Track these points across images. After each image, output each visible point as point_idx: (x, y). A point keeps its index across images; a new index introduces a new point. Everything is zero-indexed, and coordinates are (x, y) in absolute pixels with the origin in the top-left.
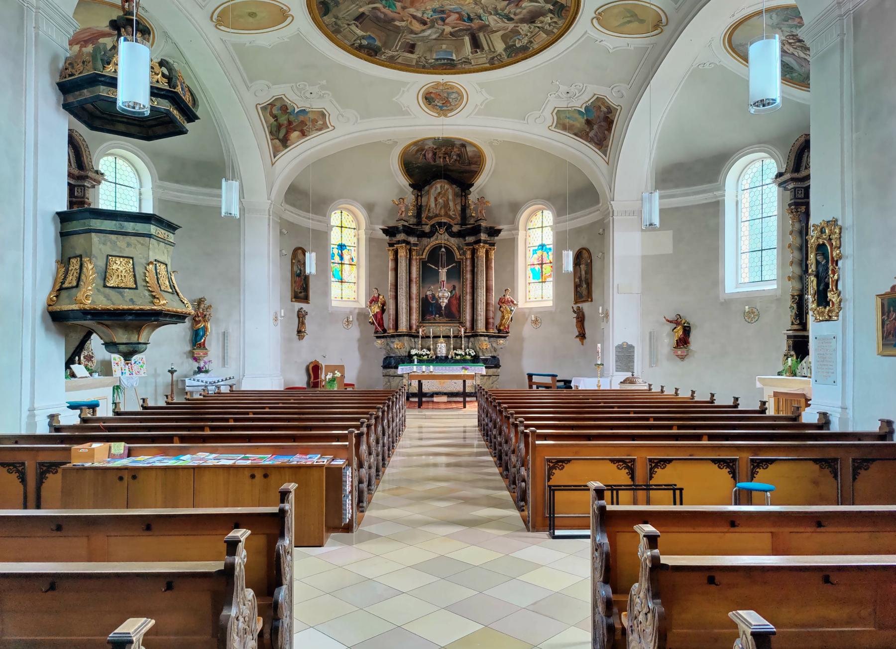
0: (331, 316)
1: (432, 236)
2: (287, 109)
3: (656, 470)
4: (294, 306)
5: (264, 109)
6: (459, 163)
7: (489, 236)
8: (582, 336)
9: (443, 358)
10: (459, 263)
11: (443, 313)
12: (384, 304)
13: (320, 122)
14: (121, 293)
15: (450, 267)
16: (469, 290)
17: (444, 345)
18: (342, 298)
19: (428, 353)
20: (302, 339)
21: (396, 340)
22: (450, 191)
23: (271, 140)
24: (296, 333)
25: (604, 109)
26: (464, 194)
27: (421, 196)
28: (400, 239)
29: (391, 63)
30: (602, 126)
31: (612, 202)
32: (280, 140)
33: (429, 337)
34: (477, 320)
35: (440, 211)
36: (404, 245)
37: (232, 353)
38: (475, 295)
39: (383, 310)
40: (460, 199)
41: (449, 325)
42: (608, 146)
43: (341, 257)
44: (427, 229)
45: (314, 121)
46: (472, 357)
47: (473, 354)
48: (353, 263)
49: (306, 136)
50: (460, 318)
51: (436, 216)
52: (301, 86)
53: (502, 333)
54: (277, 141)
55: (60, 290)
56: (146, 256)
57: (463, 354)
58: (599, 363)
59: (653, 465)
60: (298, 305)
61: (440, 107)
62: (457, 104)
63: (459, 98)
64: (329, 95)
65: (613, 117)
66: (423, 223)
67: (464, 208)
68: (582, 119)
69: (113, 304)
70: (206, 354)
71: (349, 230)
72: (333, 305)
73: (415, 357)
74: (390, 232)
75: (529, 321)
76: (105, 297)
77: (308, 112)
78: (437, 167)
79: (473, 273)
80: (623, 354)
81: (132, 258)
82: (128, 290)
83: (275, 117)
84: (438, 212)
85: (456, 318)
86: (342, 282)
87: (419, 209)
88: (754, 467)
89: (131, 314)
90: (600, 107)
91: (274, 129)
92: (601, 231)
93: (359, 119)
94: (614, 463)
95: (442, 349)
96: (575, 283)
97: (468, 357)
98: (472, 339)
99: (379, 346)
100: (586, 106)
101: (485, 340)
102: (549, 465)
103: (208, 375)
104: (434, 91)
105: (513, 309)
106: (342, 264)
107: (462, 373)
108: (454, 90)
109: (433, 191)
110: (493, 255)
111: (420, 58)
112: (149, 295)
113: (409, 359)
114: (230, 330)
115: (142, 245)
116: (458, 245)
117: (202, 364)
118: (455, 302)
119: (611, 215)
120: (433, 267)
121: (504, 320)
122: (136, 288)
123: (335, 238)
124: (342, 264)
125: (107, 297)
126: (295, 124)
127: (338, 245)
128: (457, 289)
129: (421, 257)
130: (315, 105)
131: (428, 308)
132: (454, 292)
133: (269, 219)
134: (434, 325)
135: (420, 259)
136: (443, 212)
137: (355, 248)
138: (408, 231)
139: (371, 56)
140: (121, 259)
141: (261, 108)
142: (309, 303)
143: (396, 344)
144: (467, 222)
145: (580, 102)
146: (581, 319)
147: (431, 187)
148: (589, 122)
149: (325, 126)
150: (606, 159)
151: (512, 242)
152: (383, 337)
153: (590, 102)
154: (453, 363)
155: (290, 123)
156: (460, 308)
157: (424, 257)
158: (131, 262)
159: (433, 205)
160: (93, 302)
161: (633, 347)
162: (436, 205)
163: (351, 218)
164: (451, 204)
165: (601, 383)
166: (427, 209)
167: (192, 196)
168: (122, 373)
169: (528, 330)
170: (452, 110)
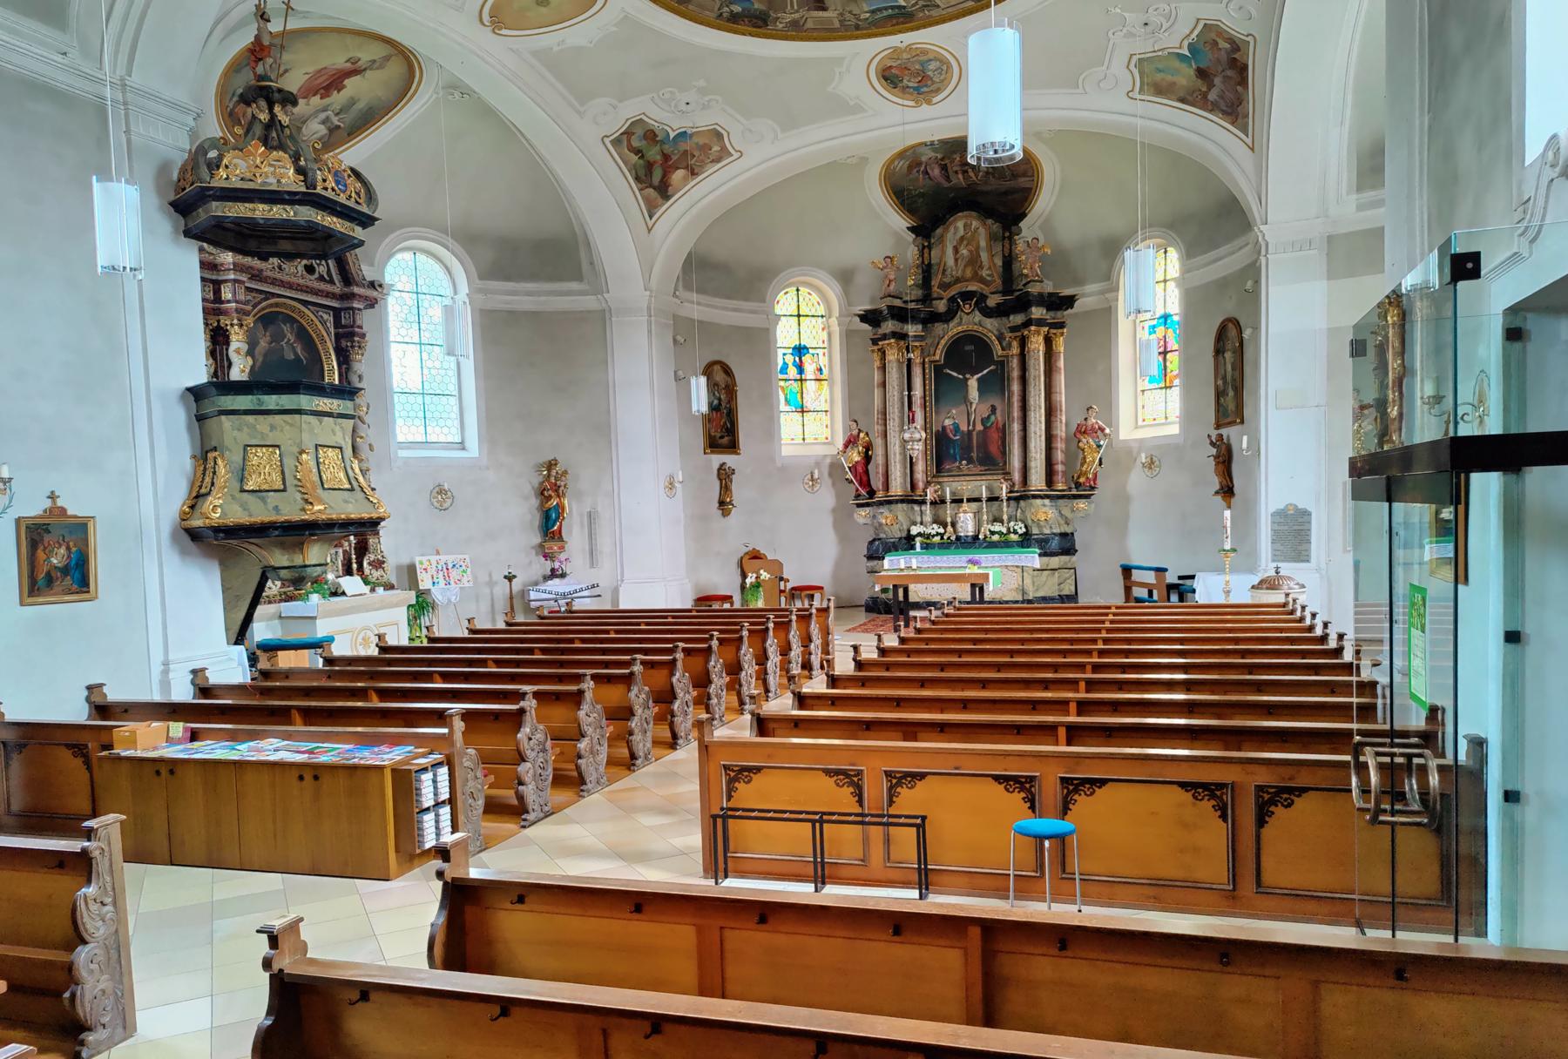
0: (784, 473)
1: (952, 318)
2: (655, 135)
3: (899, 790)
4: (710, 461)
5: (616, 142)
6: (994, 177)
7: (1047, 310)
8: (1227, 491)
10: (1002, 364)
12: (868, 447)
13: (716, 148)
14: (263, 500)
15: (985, 372)
16: (1016, 413)
17: (970, 516)
18: (804, 439)
19: (942, 531)
20: (729, 514)
21: (884, 510)
22: (982, 231)
23: (641, 190)
24: (717, 505)
25: (1224, 45)
26: (1007, 234)
27: (930, 247)
28: (887, 331)
29: (797, 31)
30: (1227, 77)
31: (1262, 227)
32: (655, 188)
35: (964, 271)
36: (893, 341)
37: (604, 543)
39: (867, 459)
40: (1001, 244)
41: (984, 478)
42: (1247, 116)
43: (800, 368)
44: (941, 306)
45: (705, 148)
48: (823, 377)
49: (697, 174)
51: (958, 280)
52: (667, 96)
53: (1082, 489)
54: (651, 190)
55: (197, 498)
56: (297, 441)
58: (1228, 546)
59: (894, 781)
60: (717, 459)
61: (914, 88)
62: (945, 79)
63: (945, 67)
64: (717, 102)
65: (1245, 57)
66: (935, 295)
67: (1009, 261)
68: (1187, 69)
69: (250, 516)
70: (562, 548)
71: (814, 319)
72: (783, 454)
73: (918, 540)
74: (871, 318)
76: (241, 506)
77: (691, 136)
78: (955, 189)
79: (1024, 380)
80: (1286, 528)
81: (278, 446)
82: (272, 493)
83: (638, 152)
84: (959, 274)
86: (803, 412)
87: (927, 271)
88: (1069, 792)
89: (276, 528)
90: (1215, 43)
91: (642, 173)
92: (1249, 284)
93: (779, 130)
94: (830, 777)
95: (967, 523)
96: (1217, 387)
97: (1013, 537)
98: (1022, 503)
99: (861, 521)
100: (1190, 44)
101: (1044, 505)
102: (729, 775)
103: (565, 580)
104: (894, 64)
105: (1102, 443)
106: (801, 380)
107: (967, 571)
108: (931, 56)
109: (950, 235)
110: (1060, 345)
111: (842, 14)
112: (303, 499)
113: (907, 543)
114: (599, 509)
115: (291, 425)
116: (998, 330)
117: (557, 565)
119: (1263, 252)
120: (955, 374)
122: (284, 490)
123: (786, 336)
124: (801, 380)
125: (244, 507)
126: (675, 158)
127: (794, 348)
129: (933, 358)
130: (701, 121)
131: (944, 451)
132: (993, 418)
133: (650, 323)
134: (957, 479)
135: (931, 362)
136: (969, 273)
137: (826, 350)
138: (900, 315)
139: (760, 27)
140: (264, 449)
141: (610, 142)
142: (739, 454)
143: (885, 516)
144: (1014, 287)
145: (1176, 37)
146: (1225, 459)
147: (947, 230)
148: (1202, 73)
149: (724, 153)
150: (1249, 141)
151: (1105, 317)
152: (867, 505)
153: (1194, 35)
154: (985, 547)
155: (666, 157)
156: (1004, 447)
157: (937, 358)
158: (278, 452)
159: (950, 261)
160: (224, 514)
161: (1309, 514)
162: (956, 260)
163: (815, 297)
164: (984, 256)
165: (1231, 586)
166: (941, 269)
167: (531, 298)
168: (434, 583)
169: (1137, 480)
170: (938, 91)
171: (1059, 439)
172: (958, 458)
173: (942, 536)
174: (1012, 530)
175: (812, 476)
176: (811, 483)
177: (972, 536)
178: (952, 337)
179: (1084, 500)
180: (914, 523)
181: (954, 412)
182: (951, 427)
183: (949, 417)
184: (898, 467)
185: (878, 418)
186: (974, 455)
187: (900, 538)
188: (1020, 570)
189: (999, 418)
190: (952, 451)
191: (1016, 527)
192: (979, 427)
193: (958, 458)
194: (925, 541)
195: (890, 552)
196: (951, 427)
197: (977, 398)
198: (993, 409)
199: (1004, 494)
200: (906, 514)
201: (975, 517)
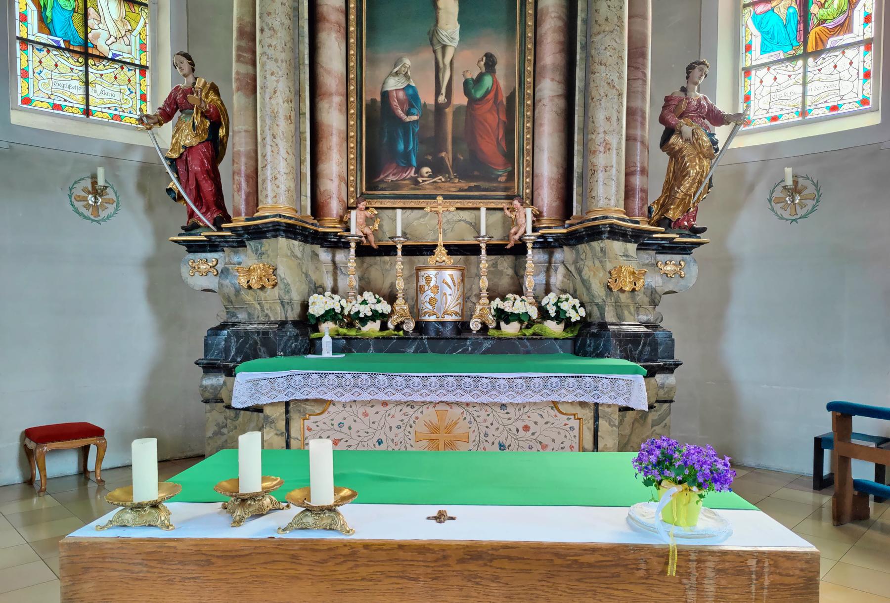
9: (448, 332)
11: (449, 162)
17: (448, 275)
18: (87, 112)
19: (384, 307)
33: (389, 250)
34: (589, 171)
38: (579, 73)
46: (569, 324)
47: (575, 317)
50: (511, 176)
57: (534, 313)
73: (327, 328)
75: (761, 191)
85: (495, 179)
97: (553, 328)
99: (200, 282)
118: (492, 119)
121: (687, 184)
128: (500, 69)
132: (488, 81)
152: (211, 246)
154: (488, 351)
156: (510, 142)
171: (639, 119)
172: (414, 163)
173: (383, 318)
174: (552, 312)
175: (94, 183)
176: (91, 199)
177: (455, 323)
179: (678, 257)
180: (319, 289)
181: (407, 62)
182: (401, 94)
183: (397, 74)
184: (283, 152)
185: (239, 48)
186: (447, 156)
187: (283, 324)
188: (589, 414)
189: (502, 83)
190: (401, 147)
191: (564, 306)
192: (460, 99)
194: (344, 331)
195: (256, 356)
197: (457, 38)
198: (490, 63)
199: (529, 232)
200: (300, 266)
201: (463, 276)
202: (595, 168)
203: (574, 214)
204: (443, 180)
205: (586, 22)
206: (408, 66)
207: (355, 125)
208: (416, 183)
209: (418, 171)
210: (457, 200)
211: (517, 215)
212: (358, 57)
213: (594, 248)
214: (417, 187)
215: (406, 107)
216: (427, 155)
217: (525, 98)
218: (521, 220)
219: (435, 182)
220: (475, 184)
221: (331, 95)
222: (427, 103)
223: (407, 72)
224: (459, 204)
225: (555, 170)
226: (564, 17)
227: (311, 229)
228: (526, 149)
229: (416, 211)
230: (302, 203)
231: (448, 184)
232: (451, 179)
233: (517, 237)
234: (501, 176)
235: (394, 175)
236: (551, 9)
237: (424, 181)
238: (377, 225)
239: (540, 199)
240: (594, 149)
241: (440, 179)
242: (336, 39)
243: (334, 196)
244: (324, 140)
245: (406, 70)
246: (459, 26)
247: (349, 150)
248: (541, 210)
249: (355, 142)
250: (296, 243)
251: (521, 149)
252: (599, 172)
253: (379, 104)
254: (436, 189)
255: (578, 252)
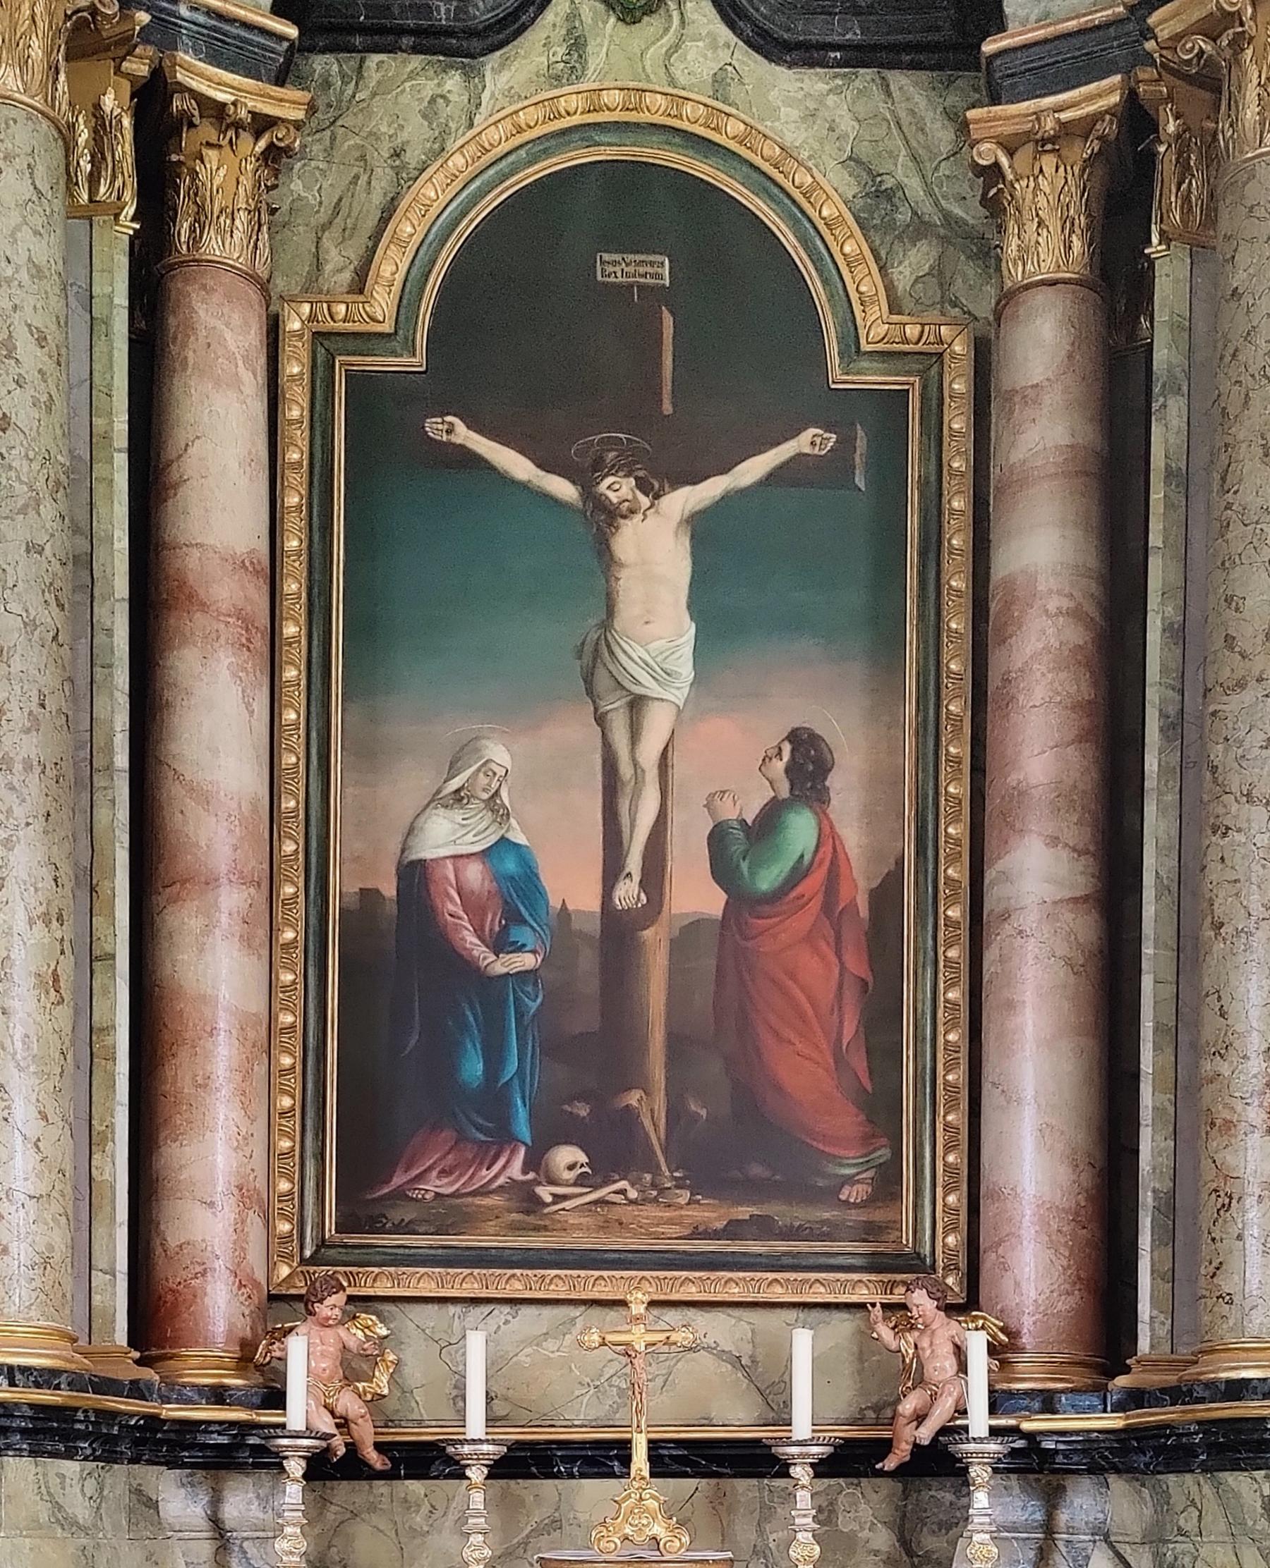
41: (734, 1286)
134: (516, 1283)
172: (522, 1128)
178: (506, 163)
181: (498, 753)
182: (474, 874)
183: (458, 798)
190: (473, 1068)
193: (522, 1128)
196: (474, 874)
197: (686, 670)
199: (979, 1421)
202: (1235, 1190)
203: (1144, 1344)
204: (633, 1194)
205: (1178, 633)
206: (500, 772)
207: (301, 987)
208: (532, 1204)
209: (534, 1162)
210: (685, 1274)
211: (925, 1343)
212: (314, 735)
213: (1237, 1496)
214: (531, 1219)
215: (493, 921)
216: (571, 1100)
217: (941, 895)
218: (941, 1365)
219: (601, 1202)
220: (754, 1210)
221: (211, 882)
222: (570, 907)
223: (497, 793)
224: (694, 1289)
225: (1064, 1174)
226: (1091, 609)
227: (131, 1415)
228: (946, 1083)
229: (528, 1312)
230: (97, 1299)
231: (653, 1212)
232: (662, 1191)
233: (925, 1434)
234: (850, 1180)
235: (444, 1173)
236: (1045, 583)
237: (558, 1198)
238: (385, 1379)
239: (1007, 1283)
240: (1226, 1115)
241: (622, 1192)
242: (234, 675)
243: (219, 1264)
244: (184, 1054)
245: (495, 785)
246: (690, 630)
247: (276, 1080)
248: (1013, 1326)
249: (299, 1052)
250: (71, 1467)
251: (928, 1080)
252: (1250, 1201)
253: (392, 909)
254: (605, 1226)
255: (1163, 1499)
